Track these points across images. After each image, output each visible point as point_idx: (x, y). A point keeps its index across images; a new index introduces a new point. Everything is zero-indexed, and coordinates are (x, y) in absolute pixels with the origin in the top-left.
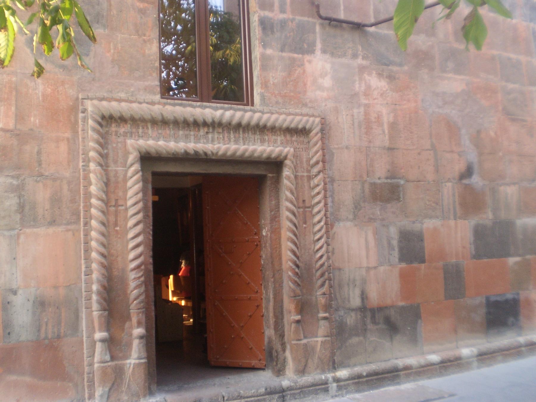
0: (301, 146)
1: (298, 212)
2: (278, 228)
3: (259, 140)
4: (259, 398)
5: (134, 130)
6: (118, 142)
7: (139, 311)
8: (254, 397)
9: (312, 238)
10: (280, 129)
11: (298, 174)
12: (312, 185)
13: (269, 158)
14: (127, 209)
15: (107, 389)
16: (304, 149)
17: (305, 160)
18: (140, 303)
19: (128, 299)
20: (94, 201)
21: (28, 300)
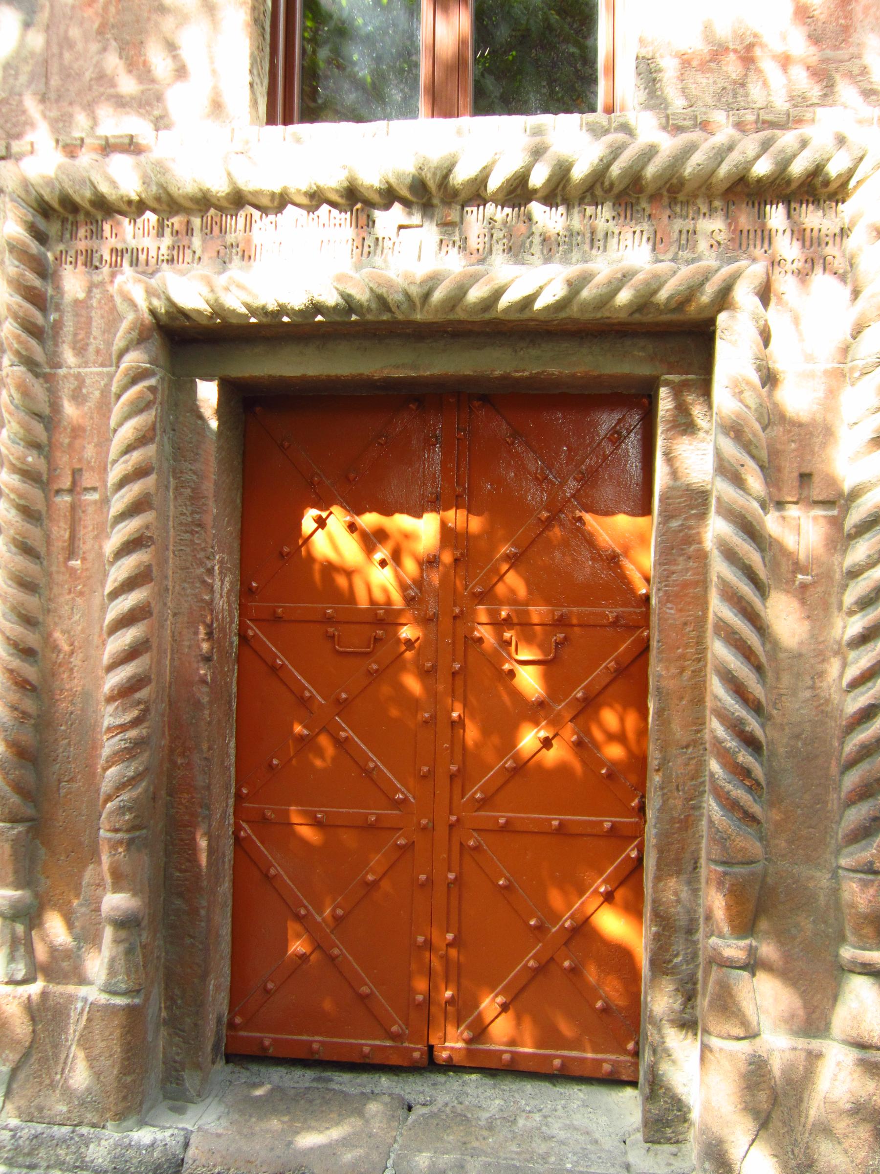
2: (696, 584)
7: (119, 836)
14: (105, 501)
18: (121, 810)
19: (98, 790)
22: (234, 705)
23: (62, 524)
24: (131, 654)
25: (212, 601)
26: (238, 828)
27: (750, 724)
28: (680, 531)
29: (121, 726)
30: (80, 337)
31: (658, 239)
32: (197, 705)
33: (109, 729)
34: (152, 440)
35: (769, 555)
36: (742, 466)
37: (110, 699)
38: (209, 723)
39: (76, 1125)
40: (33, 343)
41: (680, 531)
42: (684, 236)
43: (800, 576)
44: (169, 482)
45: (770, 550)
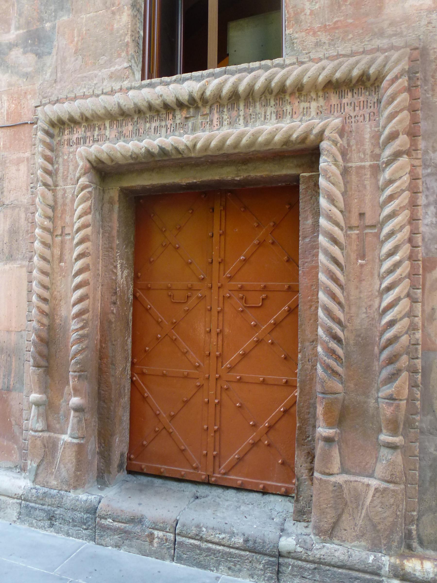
0: (361, 112)
1: (347, 236)
3: (274, 116)
4: (232, 550)
5: (89, 134)
6: (70, 153)
7: (76, 374)
8: (224, 546)
9: (377, 287)
10: (314, 86)
11: (350, 164)
12: (381, 182)
13: (287, 142)
14: (73, 239)
15: (35, 465)
16: (367, 116)
17: (367, 136)
18: (76, 363)
20: (38, 231)
22: (131, 324)
23: (58, 249)
24: (81, 300)
25: (116, 279)
26: (132, 376)
27: (334, 329)
28: (309, 243)
29: (77, 329)
30: (65, 174)
31: (294, 113)
32: (110, 322)
33: (72, 331)
34: (90, 213)
35: (345, 252)
36: (330, 210)
37: (74, 318)
38: (115, 330)
39: (60, 490)
40: (48, 177)
41: (309, 243)
42: (305, 110)
43: (360, 261)
44: (100, 231)
45: (346, 249)
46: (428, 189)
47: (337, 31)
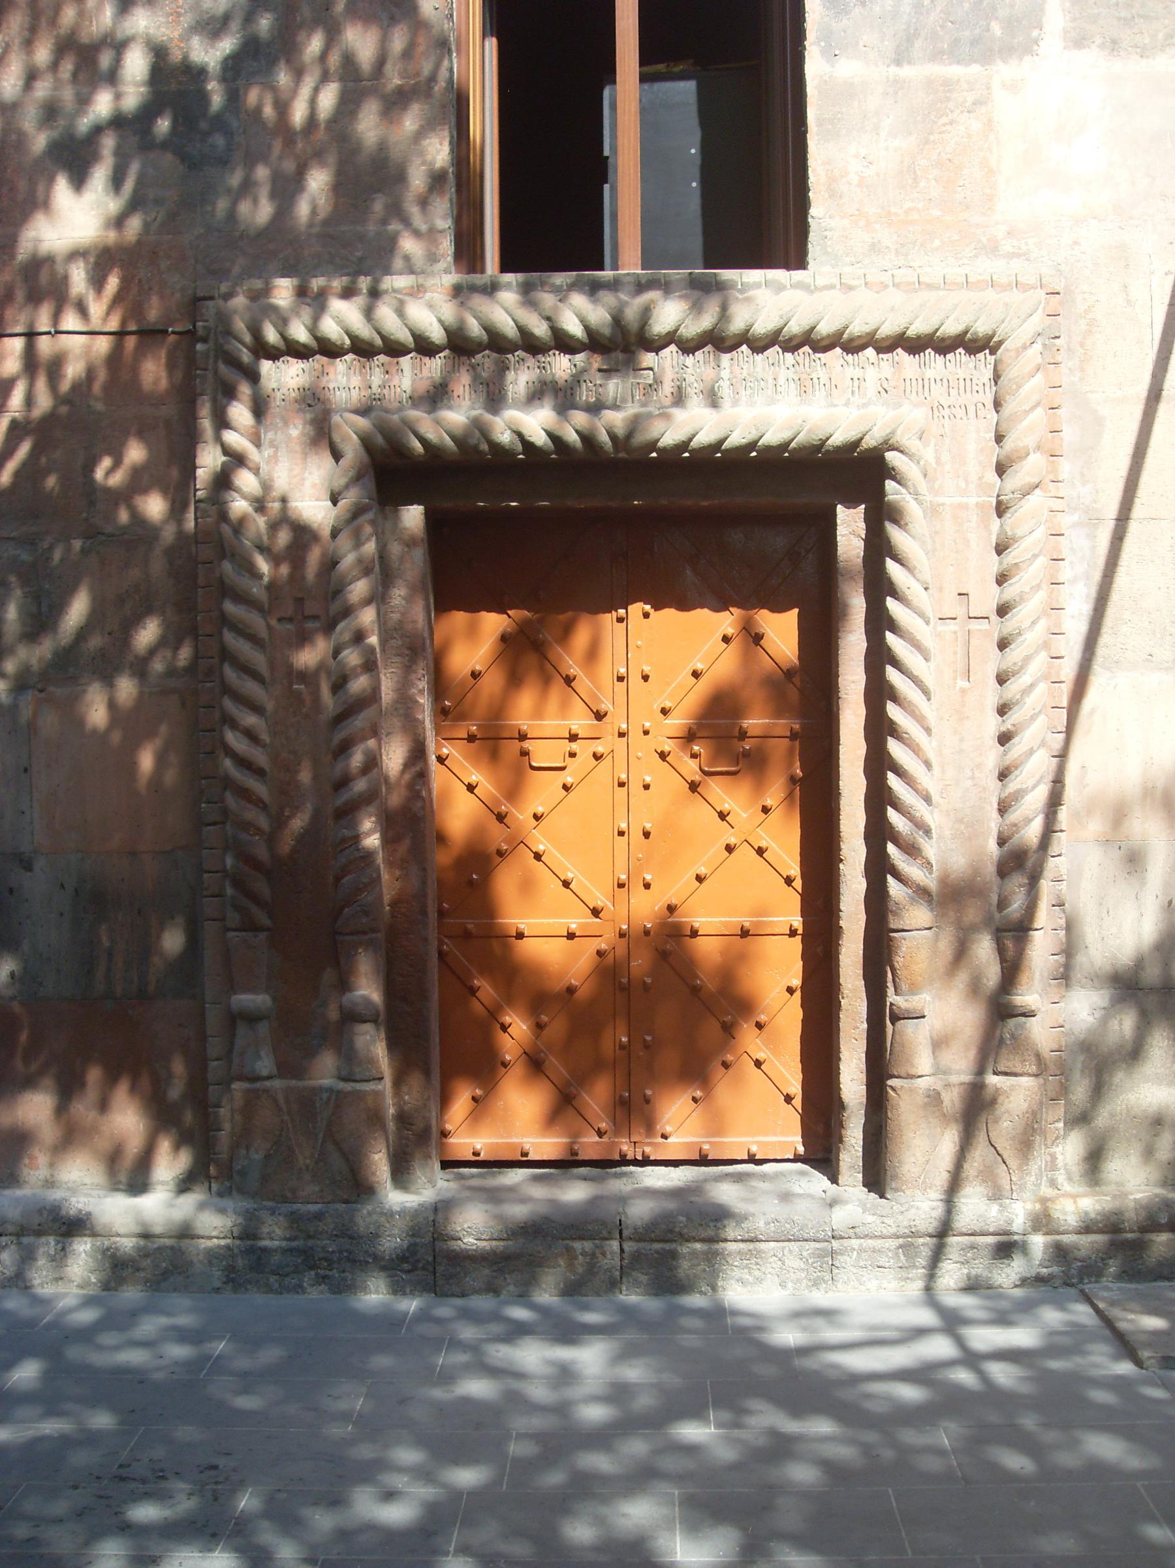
11: (940, 500)
16: (971, 410)
21: (62, 885)
26: (441, 943)
35: (932, 664)
42: (856, 383)
46: (1072, 549)
47: (911, 229)
